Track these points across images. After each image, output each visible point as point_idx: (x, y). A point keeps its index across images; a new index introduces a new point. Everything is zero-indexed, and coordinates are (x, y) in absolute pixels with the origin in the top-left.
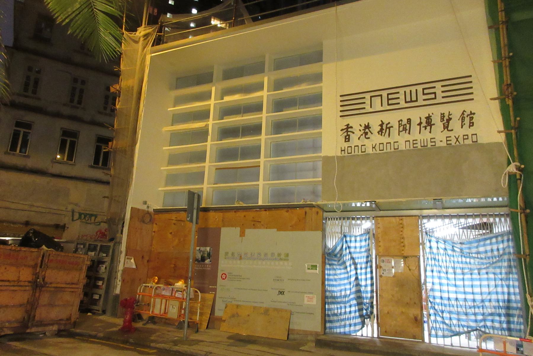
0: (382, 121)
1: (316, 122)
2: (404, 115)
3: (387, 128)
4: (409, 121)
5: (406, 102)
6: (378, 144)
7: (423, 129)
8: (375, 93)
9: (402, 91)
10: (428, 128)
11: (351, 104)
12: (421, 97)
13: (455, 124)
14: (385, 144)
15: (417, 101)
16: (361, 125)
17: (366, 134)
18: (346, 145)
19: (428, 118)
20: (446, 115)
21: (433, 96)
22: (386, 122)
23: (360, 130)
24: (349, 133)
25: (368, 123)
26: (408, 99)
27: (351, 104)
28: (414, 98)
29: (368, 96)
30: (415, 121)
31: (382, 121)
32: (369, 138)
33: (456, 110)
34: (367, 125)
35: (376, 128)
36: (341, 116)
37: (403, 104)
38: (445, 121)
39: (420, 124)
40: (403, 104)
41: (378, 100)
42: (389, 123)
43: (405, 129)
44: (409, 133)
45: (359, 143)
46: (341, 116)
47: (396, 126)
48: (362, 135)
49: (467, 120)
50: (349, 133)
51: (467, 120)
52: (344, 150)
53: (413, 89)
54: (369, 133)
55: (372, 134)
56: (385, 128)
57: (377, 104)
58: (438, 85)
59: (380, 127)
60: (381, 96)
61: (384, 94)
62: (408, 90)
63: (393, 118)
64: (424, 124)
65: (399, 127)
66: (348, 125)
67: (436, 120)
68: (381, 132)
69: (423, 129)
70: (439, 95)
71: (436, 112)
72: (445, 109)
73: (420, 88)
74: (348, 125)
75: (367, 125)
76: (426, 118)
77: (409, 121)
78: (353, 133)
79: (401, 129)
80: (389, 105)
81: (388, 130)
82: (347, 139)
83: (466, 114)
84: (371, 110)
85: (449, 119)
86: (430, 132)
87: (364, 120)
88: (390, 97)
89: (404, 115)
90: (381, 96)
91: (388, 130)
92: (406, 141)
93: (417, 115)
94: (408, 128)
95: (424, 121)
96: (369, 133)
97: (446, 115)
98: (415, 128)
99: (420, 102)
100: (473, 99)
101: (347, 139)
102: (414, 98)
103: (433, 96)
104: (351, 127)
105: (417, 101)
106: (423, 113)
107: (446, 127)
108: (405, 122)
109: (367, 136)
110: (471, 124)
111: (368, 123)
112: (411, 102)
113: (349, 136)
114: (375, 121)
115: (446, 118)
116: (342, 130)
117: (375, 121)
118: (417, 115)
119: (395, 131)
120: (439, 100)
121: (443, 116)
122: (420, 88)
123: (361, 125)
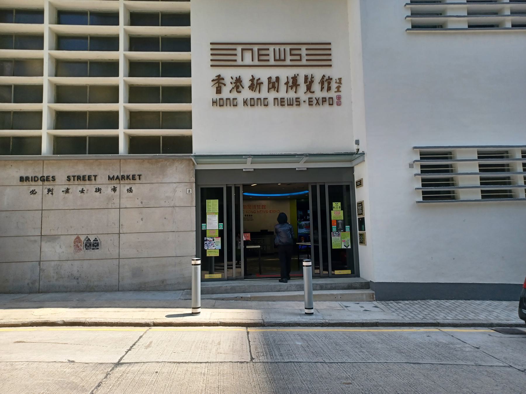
1: (183, 69)
2: (274, 73)
3: (257, 84)
4: (278, 78)
5: (275, 60)
6: (249, 99)
8: (247, 46)
9: (272, 48)
11: (223, 53)
12: (289, 57)
13: (316, 87)
14: (256, 99)
15: (284, 60)
17: (237, 87)
18: (219, 96)
20: (310, 77)
21: (298, 58)
23: (231, 83)
24: (220, 85)
26: (277, 57)
27: (223, 53)
28: (282, 57)
30: (283, 80)
32: (240, 92)
33: (318, 73)
34: (238, 78)
35: (246, 83)
36: (211, 66)
37: (272, 62)
38: (308, 83)
39: (287, 83)
41: (248, 55)
42: (259, 79)
43: (274, 87)
44: (277, 91)
45: (232, 96)
46: (211, 66)
48: (233, 88)
50: (220, 85)
52: (216, 102)
53: (282, 48)
54: (240, 87)
55: (243, 88)
56: (255, 85)
58: (304, 48)
59: (251, 83)
60: (252, 50)
61: (256, 48)
62: (277, 48)
63: (264, 74)
64: (290, 84)
65: (269, 84)
67: (301, 80)
68: (252, 87)
69: (289, 89)
70: (305, 58)
71: (302, 72)
72: (308, 71)
74: (219, 76)
75: (238, 78)
76: (292, 78)
77: (278, 78)
78: (225, 85)
79: (271, 86)
80: (259, 60)
81: (258, 86)
82: (219, 91)
83: (325, 79)
85: (312, 82)
86: (296, 92)
87: (235, 72)
88: (261, 53)
89: (274, 73)
90: (252, 50)
91: (258, 86)
92: (274, 99)
93: (284, 74)
95: (291, 81)
96: (240, 87)
97: (310, 77)
98: (283, 88)
100: (331, 66)
101: (219, 91)
103: (298, 58)
104: (223, 79)
105: (284, 60)
106: (290, 72)
107: (309, 88)
108: (274, 79)
109: (238, 90)
110: (329, 89)
112: (280, 61)
113: (220, 87)
114: (246, 75)
115: (309, 80)
116: (213, 81)
117: (246, 75)
118: (284, 74)
119: (265, 87)
120: (304, 62)
121: (306, 77)
122: (288, 48)
123: (232, 78)
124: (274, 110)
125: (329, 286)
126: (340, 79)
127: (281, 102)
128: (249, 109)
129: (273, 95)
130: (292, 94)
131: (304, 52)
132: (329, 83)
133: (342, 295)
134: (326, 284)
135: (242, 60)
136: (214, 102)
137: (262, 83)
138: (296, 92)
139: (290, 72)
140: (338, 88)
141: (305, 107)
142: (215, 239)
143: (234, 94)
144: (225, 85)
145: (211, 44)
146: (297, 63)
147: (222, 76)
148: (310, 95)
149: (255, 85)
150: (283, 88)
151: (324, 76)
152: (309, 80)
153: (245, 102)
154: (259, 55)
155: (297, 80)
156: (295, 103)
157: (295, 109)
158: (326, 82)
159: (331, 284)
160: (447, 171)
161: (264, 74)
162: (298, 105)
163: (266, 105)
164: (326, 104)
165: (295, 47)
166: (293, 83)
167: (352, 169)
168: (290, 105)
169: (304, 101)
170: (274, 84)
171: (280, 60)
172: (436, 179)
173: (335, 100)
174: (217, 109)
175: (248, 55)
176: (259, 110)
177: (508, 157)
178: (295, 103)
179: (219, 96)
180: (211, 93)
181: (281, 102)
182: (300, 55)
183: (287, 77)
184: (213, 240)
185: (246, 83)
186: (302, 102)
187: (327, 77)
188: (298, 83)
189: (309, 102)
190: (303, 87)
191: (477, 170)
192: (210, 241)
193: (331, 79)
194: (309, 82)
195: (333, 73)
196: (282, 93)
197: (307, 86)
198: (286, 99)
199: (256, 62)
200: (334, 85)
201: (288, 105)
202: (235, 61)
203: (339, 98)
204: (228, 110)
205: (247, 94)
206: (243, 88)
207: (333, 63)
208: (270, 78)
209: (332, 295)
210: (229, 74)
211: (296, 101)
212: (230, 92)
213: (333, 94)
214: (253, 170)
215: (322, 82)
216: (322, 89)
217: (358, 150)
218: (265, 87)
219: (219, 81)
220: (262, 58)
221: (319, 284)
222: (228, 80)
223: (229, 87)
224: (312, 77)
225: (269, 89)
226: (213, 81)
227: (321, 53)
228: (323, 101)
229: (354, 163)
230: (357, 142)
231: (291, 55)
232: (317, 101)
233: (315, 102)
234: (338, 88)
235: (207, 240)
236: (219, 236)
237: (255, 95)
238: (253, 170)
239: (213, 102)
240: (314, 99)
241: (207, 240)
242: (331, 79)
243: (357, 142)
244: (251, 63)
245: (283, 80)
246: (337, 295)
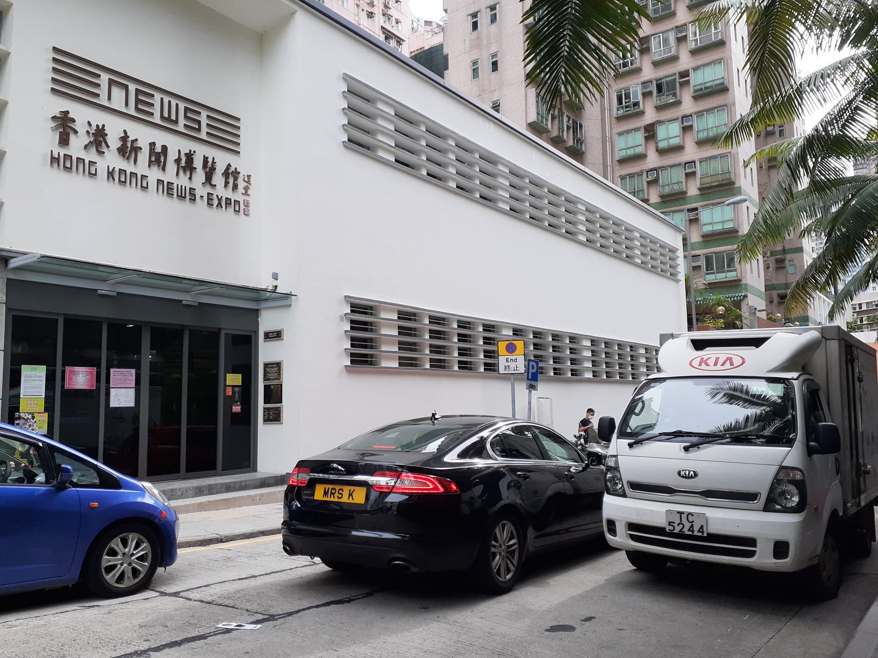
0: (125, 131)
4: (165, 148)
5: (162, 117)
6: (117, 170)
7: (181, 172)
8: (119, 79)
9: (158, 96)
10: (188, 173)
11: (73, 75)
12: (182, 121)
13: (218, 179)
15: (176, 122)
16: (89, 123)
18: (63, 152)
19: (190, 156)
22: (130, 139)
23: (88, 132)
25: (103, 126)
28: (173, 117)
29: (105, 77)
31: (125, 131)
33: (222, 160)
35: (114, 141)
36: (52, 89)
37: (157, 119)
39: (178, 161)
40: (157, 119)
42: (136, 140)
44: (164, 169)
47: (146, 151)
49: (231, 180)
51: (231, 180)
52: (58, 159)
53: (174, 103)
57: (118, 100)
58: (204, 114)
62: (166, 99)
63: (143, 135)
64: (183, 163)
66: (68, 112)
67: (198, 163)
68: (122, 151)
69: (181, 172)
70: (204, 129)
71: (201, 152)
72: (211, 153)
73: (182, 106)
74: (68, 112)
79: (153, 159)
80: (137, 109)
82: (64, 141)
83: (230, 171)
84: (106, 104)
85: (213, 169)
86: (190, 178)
87: (99, 118)
89: (161, 138)
90: (126, 87)
93: (176, 146)
94: (162, 160)
99: (181, 128)
100: (239, 153)
101: (64, 141)
102: (173, 117)
104: (73, 120)
108: (158, 149)
110: (235, 187)
111: (103, 126)
113: (68, 135)
115: (210, 164)
117: (115, 128)
121: (206, 160)
122: (182, 106)
123: (89, 123)
124: (155, 200)
125: (238, 485)
126: (249, 176)
127: (168, 189)
128: (114, 188)
129: (154, 174)
130: (183, 181)
131: (204, 121)
132: (236, 179)
133: (261, 495)
134: (235, 483)
135: (109, 98)
136: (54, 160)
137: (141, 148)
138: (190, 178)
139: (186, 146)
140: (246, 189)
141: (202, 204)
142: (35, 415)
143: (90, 156)
144: (76, 132)
145: (55, 49)
146: (192, 133)
147: (71, 115)
148: (209, 189)
149: (128, 149)
150: (171, 167)
151: (229, 165)
152: (210, 164)
153: (111, 174)
154: (138, 101)
155: (192, 159)
156: (188, 197)
157: (186, 205)
158: (231, 174)
159: (241, 482)
160: (366, 330)
161: (143, 135)
162: (193, 199)
163: (145, 188)
164: (231, 210)
165: (193, 108)
166: (187, 165)
167: (256, 312)
168: (181, 196)
169: (202, 197)
170: (158, 157)
171: (169, 120)
172: (360, 337)
173: (242, 206)
174: (58, 175)
175: (118, 94)
176: (131, 193)
177: (415, 320)
178: (188, 197)
179: (63, 152)
180: (49, 141)
181: (168, 188)
182: (199, 122)
183: (179, 151)
184: (33, 418)
185: (114, 141)
186: (198, 197)
187: (232, 169)
188: (195, 165)
189: (209, 199)
190: (200, 176)
191: (395, 332)
192: (26, 420)
193: (239, 173)
194: (210, 171)
195: (239, 163)
196: (170, 174)
197: (206, 173)
198: (175, 185)
199: (132, 112)
200: (241, 184)
201: (178, 195)
202: (98, 95)
203: (247, 205)
204: (77, 181)
205: (112, 159)
206: (108, 147)
207: (241, 149)
208: (152, 145)
209: (250, 496)
210: (83, 116)
211: (190, 193)
212: (86, 147)
213: (238, 196)
214: (115, 294)
215: (226, 174)
216: (226, 184)
217: (276, 287)
218: (144, 156)
219: (64, 125)
220: (140, 107)
221: (226, 484)
222: (80, 126)
223: (86, 140)
224: (213, 163)
225: (150, 163)
226: (54, 118)
227: (225, 130)
228: (226, 204)
229: (263, 305)
230: (275, 277)
231: (186, 117)
232: (220, 200)
233: (216, 202)
234: (246, 189)
235: (19, 418)
236: (46, 410)
237: (129, 168)
238: (115, 294)
239: (52, 158)
240: (215, 196)
241: (19, 418)
242: (239, 173)
243: (275, 277)
244: (124, 110)
245: (172, 156)
246: (256, 496)
